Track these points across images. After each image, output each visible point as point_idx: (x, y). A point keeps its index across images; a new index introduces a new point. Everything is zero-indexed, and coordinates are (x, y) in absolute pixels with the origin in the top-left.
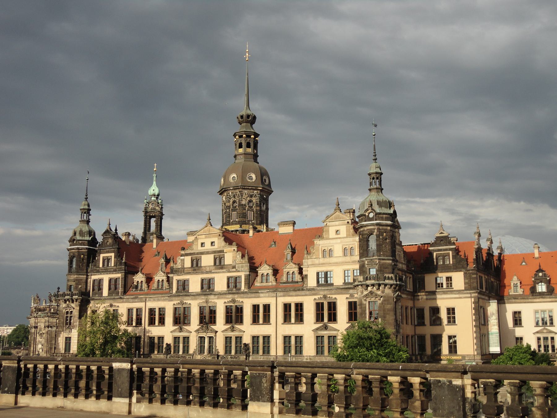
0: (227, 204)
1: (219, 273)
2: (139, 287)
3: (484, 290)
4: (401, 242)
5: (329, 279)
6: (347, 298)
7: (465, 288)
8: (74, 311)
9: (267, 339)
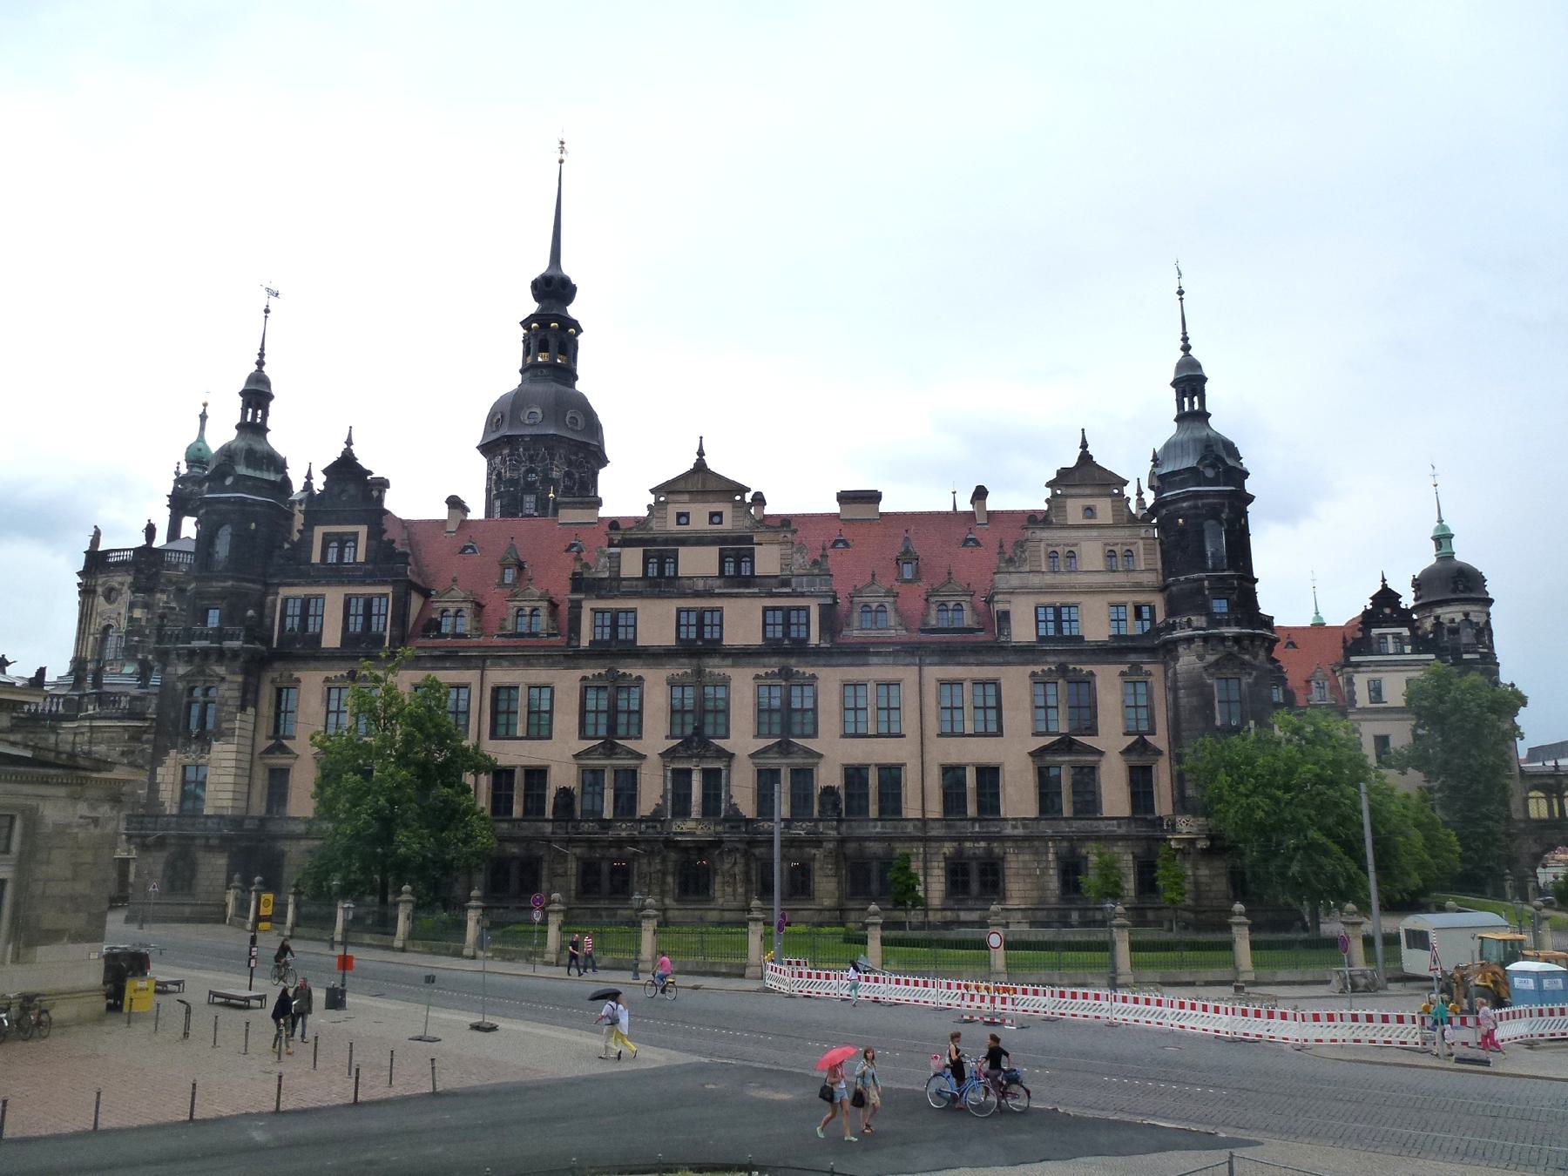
2: (445, 629)
5: (1065, 625)
6: (1122, 674)
9: (891, 775)
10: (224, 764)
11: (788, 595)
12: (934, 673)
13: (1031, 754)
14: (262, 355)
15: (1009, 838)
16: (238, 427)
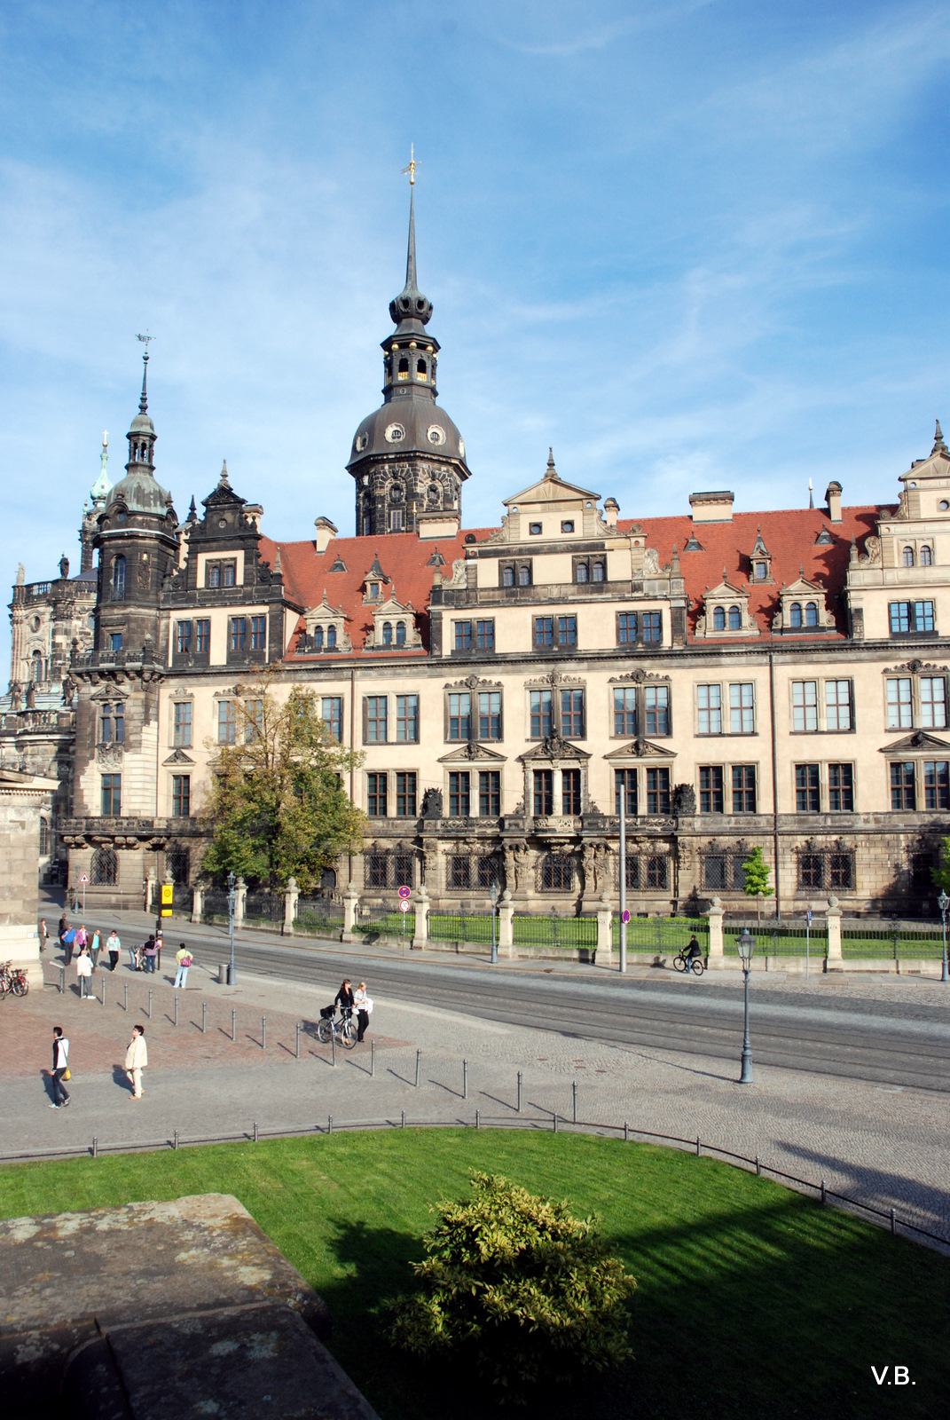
1: (591, 602)
5: (919, 621)
8: (128, 703)
10: (135, 772)
11: (640, 599)
12: (786, 671)
13: (881, 750)
14: (144, 400)
15: (860, 832)
16: (127, 467)
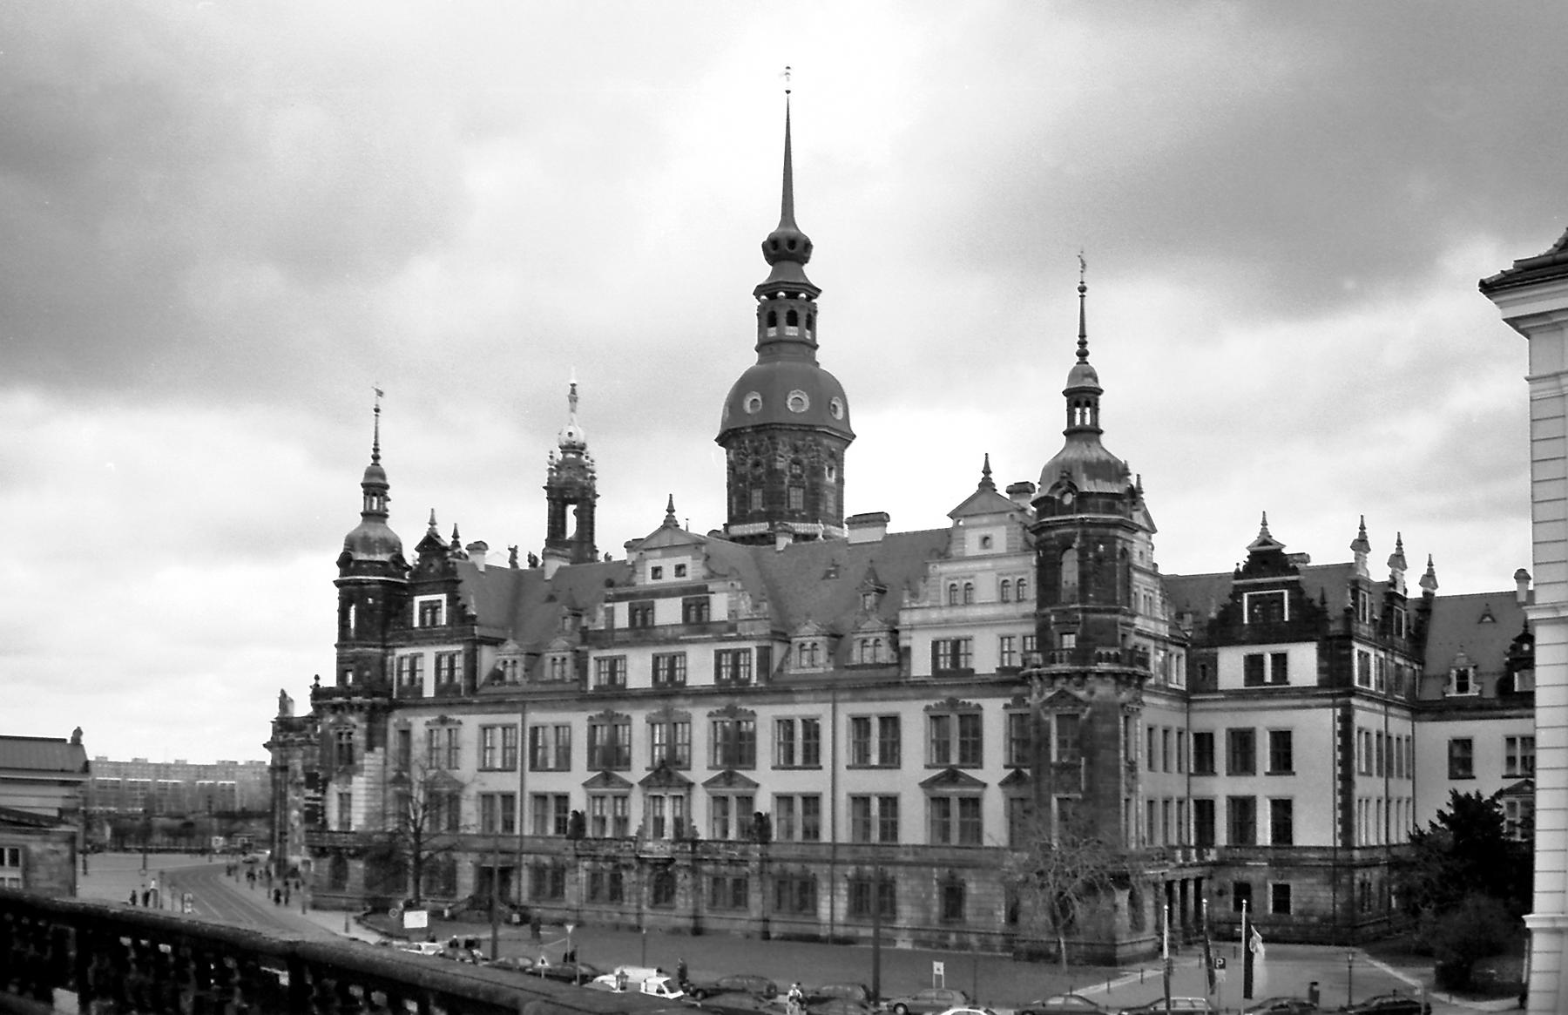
0: (741, 470)
2: (508, 678)
3: (1373, 688)
4: (1155, 565)
5: (962, 658)
7: (1320, 681)
8: (356, 732)
